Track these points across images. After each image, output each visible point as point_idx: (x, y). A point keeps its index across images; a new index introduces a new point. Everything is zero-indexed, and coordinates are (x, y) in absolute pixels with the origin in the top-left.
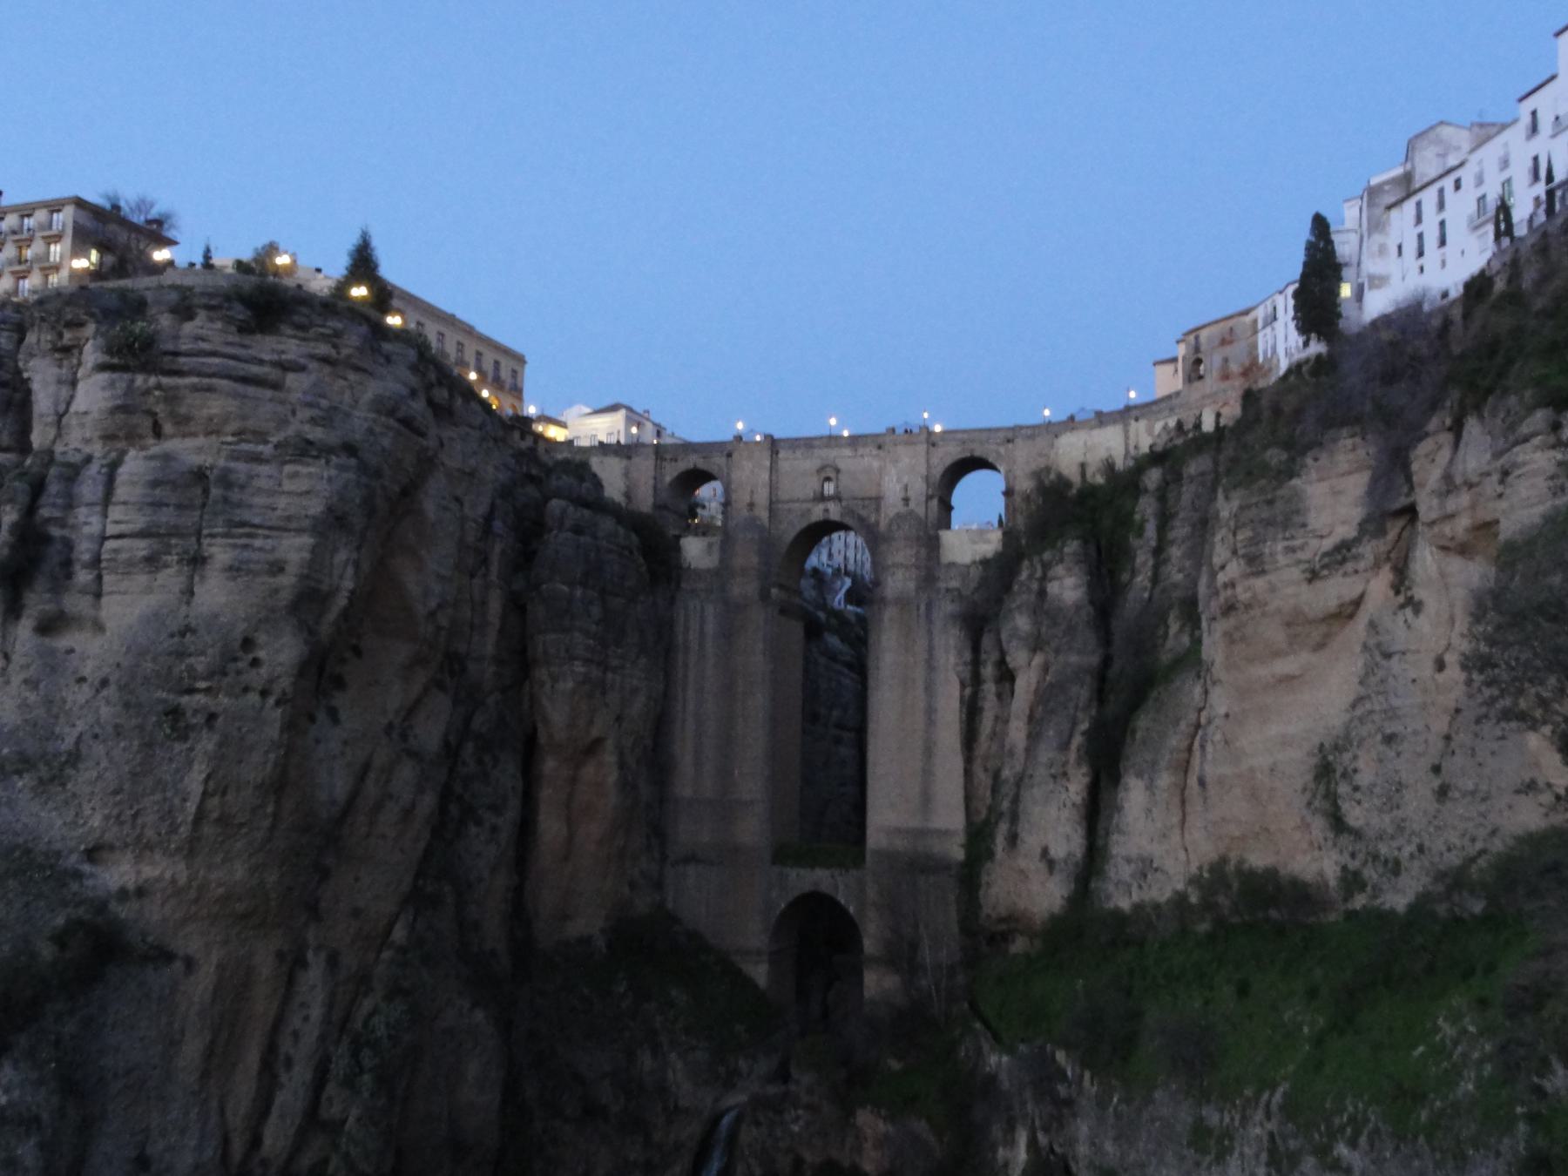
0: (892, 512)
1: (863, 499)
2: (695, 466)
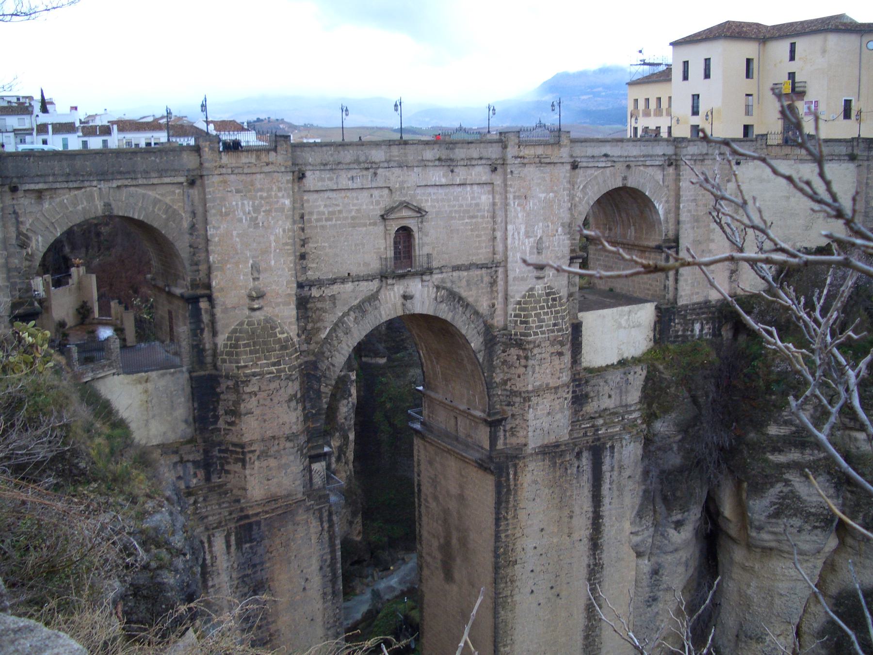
0: (517, 292)
1: (468, 268)
2: (107, 205)
